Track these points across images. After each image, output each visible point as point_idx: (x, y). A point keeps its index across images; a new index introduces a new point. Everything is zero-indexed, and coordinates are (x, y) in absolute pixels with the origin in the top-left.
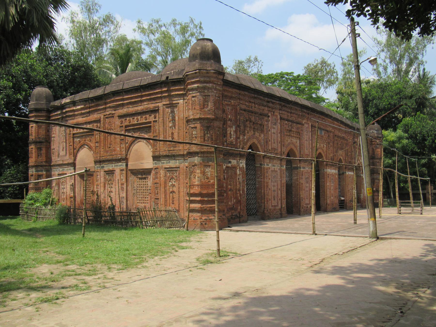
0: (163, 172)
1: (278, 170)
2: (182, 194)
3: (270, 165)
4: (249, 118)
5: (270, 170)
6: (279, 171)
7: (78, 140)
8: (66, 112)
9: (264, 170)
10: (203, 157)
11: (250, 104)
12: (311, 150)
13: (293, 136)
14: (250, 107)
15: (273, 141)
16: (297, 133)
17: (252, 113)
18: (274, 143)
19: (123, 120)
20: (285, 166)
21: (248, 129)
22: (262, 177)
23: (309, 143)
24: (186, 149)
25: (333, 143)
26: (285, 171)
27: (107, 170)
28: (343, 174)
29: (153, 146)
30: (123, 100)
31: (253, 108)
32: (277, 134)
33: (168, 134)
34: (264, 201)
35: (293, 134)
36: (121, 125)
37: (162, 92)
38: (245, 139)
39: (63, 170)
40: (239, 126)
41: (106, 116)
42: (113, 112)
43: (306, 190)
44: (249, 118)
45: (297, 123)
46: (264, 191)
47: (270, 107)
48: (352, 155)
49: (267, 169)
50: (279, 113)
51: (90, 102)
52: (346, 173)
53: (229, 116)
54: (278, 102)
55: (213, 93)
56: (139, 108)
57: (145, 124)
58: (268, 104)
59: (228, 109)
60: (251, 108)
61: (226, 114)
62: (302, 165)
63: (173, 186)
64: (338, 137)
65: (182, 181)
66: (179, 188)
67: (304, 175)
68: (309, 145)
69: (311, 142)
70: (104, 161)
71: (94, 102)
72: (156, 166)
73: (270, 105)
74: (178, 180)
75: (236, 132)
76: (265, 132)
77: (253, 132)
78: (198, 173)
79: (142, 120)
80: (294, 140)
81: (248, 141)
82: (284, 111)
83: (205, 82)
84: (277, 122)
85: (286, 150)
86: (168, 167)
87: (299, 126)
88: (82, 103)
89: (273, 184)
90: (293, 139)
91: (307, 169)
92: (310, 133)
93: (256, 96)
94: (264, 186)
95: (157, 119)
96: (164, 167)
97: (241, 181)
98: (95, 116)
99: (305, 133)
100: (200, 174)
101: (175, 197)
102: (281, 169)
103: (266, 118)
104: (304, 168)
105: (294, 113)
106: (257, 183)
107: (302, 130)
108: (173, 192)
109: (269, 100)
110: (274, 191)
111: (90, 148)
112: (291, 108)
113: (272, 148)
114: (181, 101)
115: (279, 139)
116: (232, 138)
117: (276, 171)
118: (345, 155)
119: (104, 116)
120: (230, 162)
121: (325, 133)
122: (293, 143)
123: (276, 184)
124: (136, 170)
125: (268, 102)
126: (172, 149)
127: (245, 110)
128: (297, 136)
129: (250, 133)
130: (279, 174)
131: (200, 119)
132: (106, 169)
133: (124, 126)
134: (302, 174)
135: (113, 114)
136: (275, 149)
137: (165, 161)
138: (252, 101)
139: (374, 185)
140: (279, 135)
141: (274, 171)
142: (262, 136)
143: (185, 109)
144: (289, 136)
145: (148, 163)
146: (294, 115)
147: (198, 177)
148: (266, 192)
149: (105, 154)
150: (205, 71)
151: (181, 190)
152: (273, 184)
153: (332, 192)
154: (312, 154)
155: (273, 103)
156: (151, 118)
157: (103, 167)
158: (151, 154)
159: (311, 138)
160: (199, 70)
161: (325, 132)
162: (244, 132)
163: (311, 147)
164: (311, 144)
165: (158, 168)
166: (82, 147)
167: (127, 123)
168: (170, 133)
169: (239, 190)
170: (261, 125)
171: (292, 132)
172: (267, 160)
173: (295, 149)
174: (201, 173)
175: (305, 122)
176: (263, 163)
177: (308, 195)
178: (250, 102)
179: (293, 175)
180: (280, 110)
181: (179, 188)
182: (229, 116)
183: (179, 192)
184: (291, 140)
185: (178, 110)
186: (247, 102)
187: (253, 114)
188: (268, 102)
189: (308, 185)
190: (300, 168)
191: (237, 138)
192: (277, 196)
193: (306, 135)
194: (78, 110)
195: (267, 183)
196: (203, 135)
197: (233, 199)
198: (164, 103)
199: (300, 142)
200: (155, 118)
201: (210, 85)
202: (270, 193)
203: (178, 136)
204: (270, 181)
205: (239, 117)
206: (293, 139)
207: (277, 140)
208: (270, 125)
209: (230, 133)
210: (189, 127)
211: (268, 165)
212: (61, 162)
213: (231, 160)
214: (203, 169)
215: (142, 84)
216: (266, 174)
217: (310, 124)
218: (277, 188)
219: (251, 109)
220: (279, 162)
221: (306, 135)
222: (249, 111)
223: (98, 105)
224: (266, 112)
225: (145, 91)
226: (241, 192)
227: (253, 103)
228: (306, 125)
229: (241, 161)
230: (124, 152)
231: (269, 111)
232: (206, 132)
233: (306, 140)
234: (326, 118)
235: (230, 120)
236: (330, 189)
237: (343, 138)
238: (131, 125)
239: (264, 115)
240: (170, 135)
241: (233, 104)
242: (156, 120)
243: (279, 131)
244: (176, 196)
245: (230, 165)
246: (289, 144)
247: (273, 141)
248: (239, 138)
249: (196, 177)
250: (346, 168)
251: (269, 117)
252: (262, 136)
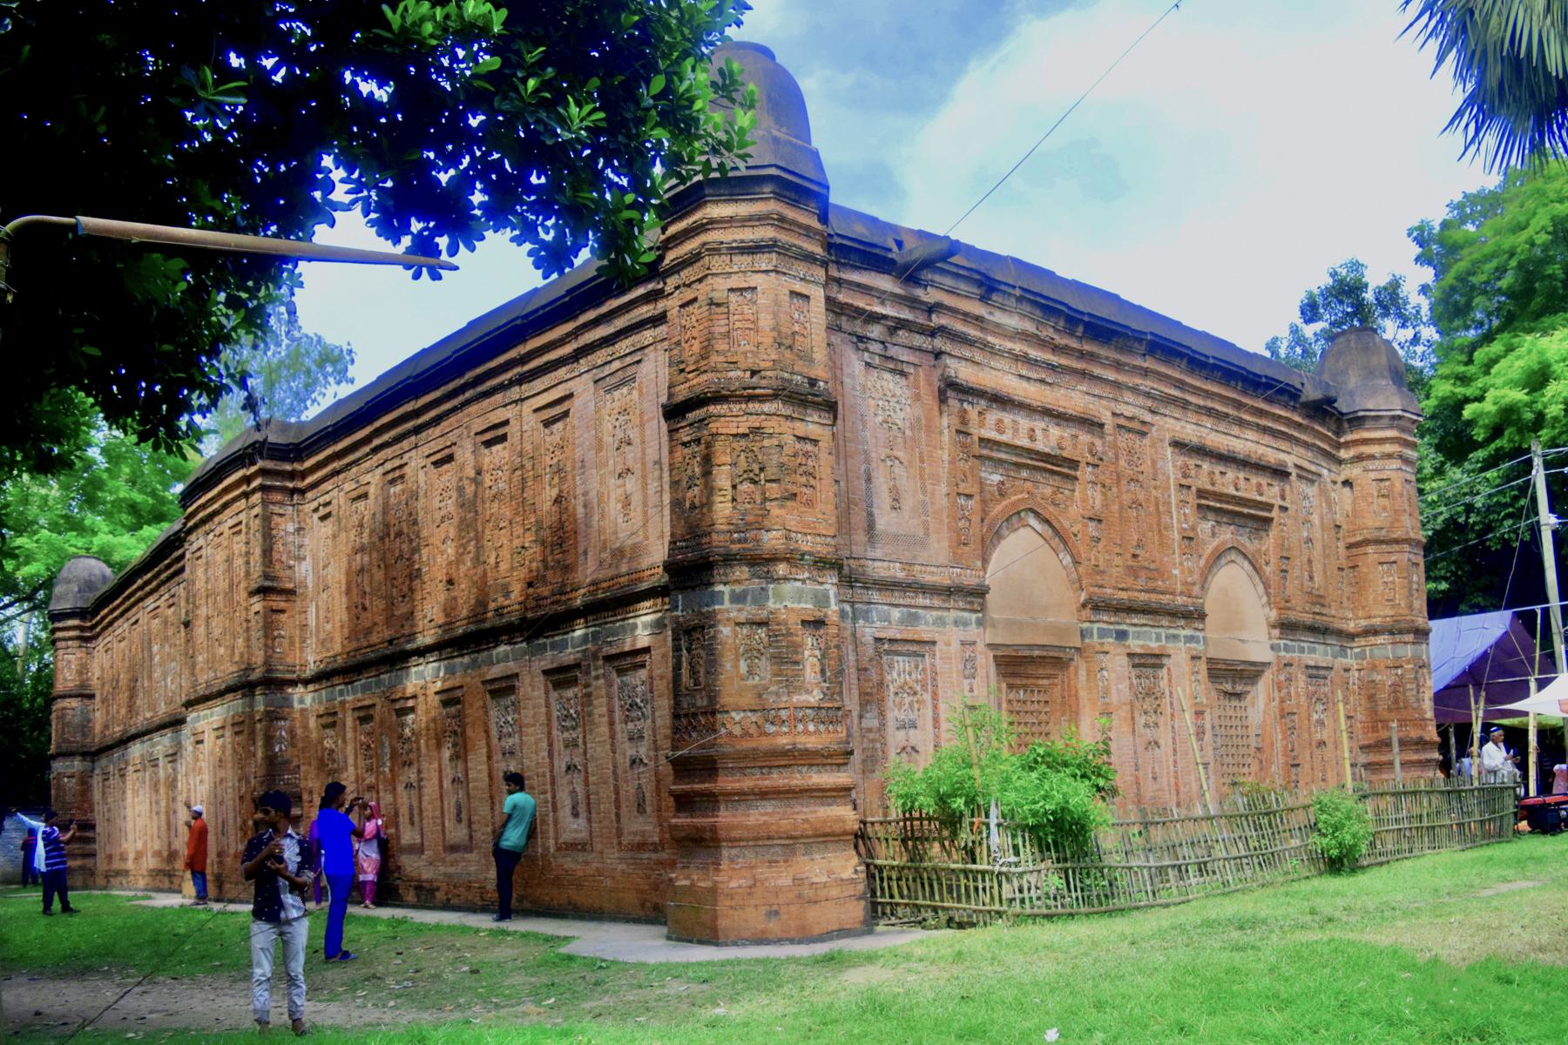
7: (996, 478)
8: (931, 309)
27: (1138, 651)
36: (1184, 482)
39: (913, 619)
41: (1122, 421)
42: (1148, 417)
51: (1062, 323)
70: (1130, 609)
71: (1072, 334)
86: (1312, 663)
88: (1027, 308)
98: (1074, 398)
111: (1060, 536)
119: (1114, 414)
124: (1225, 661)
132: (1135, 645)
133: (1194, 489)
135: (1144, 423)
137: (1305, 645)
145: (1258, 644)
149: (1130, 582)
156: (1271, 492)
157: (1122, 635)
166: (1014, 517)
167: (1203, 482)
194: (999, 330)
212: (901, 575)
223: (1091, 357)
225: (1244, 392)
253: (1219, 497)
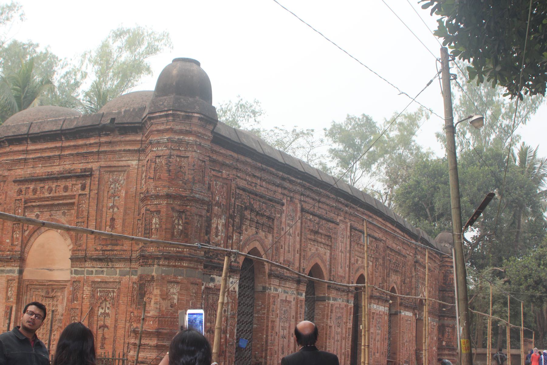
0: (89, 289)
1: (292, 300)
2: (121, 332)
3: (280, 290)
4: (250, 203)
5: (279, 300)
6: (293, 303)
9: (269, 299)
10: (168, 266)
11: (254, 180)
12: (347, 269)
13: (321, 243)
14: (253, 185)
15: (286, 248)
16: (327, 238)
17: (256, 195)
18: (289, 252)
19: (23, 187)
20: (304, 294)
21: (248, 223)
22: (266, 311)
23: (346, 256)
24: (135, 249)
25: (384, 258)
26: (303, 303)
28: (396, 314)
29: (76, 240)
30: (27, 152)
31: (258, 187)
32: (295, 237)
33: (104, 221)
34: (266, 354)
35: (321, 238)
36: (19, 198)
37: (100, 144)
38: (240, 241)
40: (232, 217)
42: (6, 174)
43: (336, 338)
44: (250, 203)
45: (328, 220)
46: (267, 336)
47: (285, 188)
48: (411, 282)
49: (274, 297)
50: (301, 201)
52: (400, 312)
53: (217, 198)
54: (299, 181)
55: (194, 153)
56: (56, 169)
57: (63, 199)
58: (282, 182)
59: (216, 185)
60: (255, 186)
61: (212, 194)
62: (333, 294)
63: (106, 315)
64: (392, 250)
65: (123, 308)
66: (116, 321)
67: (334, 311)
68: (345, 259)
69: (348, 255)
72: (77, 276)
73: (287, 184)
74: (115, 304)
75: (226, 226)
76: (275, 232)
77: (254, 230)
78: (156, 296)
79: (58, 189)
80: (322, 250)
81: (245, 244)
82: (308, 196)
83: (181, 132)
84: (296, 215)
85: (308, 266)
86: (99, 280)
87: (331, 225)
89: (282, 324)
90: (319, 248)
91: (340, 301)
92: (348, 240)
93: (264, 166)
94: (267, 326)
95: (87, 191)
96: (91, 279)
97: (229, 316)
99: (340, 239)
100: (159, 298)
101: (107, 336)
102: (297, 299)
103: (279, 207)
104: (335, 299)
105: (323, 203)
106: (255, 321)
107: (336, 233)
108: (105, 326)
109: (286, 176)
110: (284, 337)
112: (319, 194)
113: (284, 261)
114: (135, 163)
115: (298, 246)
116: (219, 237)
117: (289, 302)
118: (401, 281)
120: (213, 280)
121: (371, 241)
122: (319, 254)
123: (287, 325)
125: (283, 179)
126: (109, 248)
127: (244, 190)
128: (327, 242)
129: (249, 230)
130: (293, 307)
131: (168, 196)
133: (23, 200)
134: (332, 310)
135: (4, 176)
136: (289, 262)
137: (94, 270)
138: (258, 174)
139: (443, 336)
140: (298, 238)
141: (286, 300)
142: (270, 237)
143: (139, 177)
144: (314, 241)
145: (62, 271)
146: (325, 206)
147: (156, 303)
148: (269, 338)
150: (183, 114)
151: (121, 324)
152: (282, 324)
153: (378, 344)
154: (349, 277)
155: (291, 182)
158: (69, 254)
159: (348, 249)
160: (173, 110)
161: (371, 239)
162: (240, 227)
163: (348, 263)
164: (348, 258)
165: (79, 282)
167: (30, 195)
168: (108, 219)
170: (269, 218)
171: (319, 236)
172: (276, 282)
173: (322, 266)
174: (161, 295)
175: (340, 220)
176: (267, 285)
177: (339, 347)
178: (254, 176)
179: (316, 311)
180: (302, 194)
181: (116, 321)
182: (217, 198)
183: (115, 327)
184: (317, 249)
185: (128, 177)
186: (250, 175)
187: (258, 198)
188: (283, 179)
189: (339, 330)
190: (329, 299)
191: (229, 237)
192: (289, 346)
193: (342, 243)
195: (273, 322)
196: (169, 226)
198: (103, 164)
199: (331, 254)
200: (83, 188)
201: (191, 138)
202: (277, 340)
203: (123, 225)
204: (278, 319)
205: (233, 200)
206: (319, 248)
207: (294, 247)
208: (283, 220)
209: (217, 228)
210: (146, 210)
211: (277, 290)
213: (215, 276)
214: (165, 289)
215: (64, 127)
216: (272, 306)
217: (349, 224)
218: (289, 333)
219: (254, 189)
220: (295, 285)
221: (342, 243)
222: (251, 192)
224: (280, 197)
226: (228, 336)
227: (258, 177)
228: (342, 226)
229: (231, 280)
230: (18, 248)
231: (284, 194)
232: (176, 221)
233: (341, 252)
234: (374, 217)
235: (218, 204)
236: (375, 340)
237: (399, 253)
238: (36, 199)
239: (275, 202)
240: (109, 223)
241: (224, 176)
242: (83, 192)
243: (298, 231)
244: (109, 334)
245: (211, 285)
246: (313, 256)
247: (286, 248)
248: (231, 238)
249: (152, 302)
250: (401, 304)
251: (283, 205)
252: (270, 237)
253: (40, 199)
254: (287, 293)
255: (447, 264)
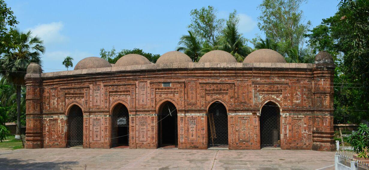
75: (57, 101)
80: (122, 97)
113: (93, 106)
169: (59, 131)
177: (145, 134)
180: (102, 80)
189: (144, 127)
197: (55, 135)
217: (149, 82)
218: (100, 130)
235: (53, 96)
248: (59, 104)
254: (98, 116)
255: (315, 75)
